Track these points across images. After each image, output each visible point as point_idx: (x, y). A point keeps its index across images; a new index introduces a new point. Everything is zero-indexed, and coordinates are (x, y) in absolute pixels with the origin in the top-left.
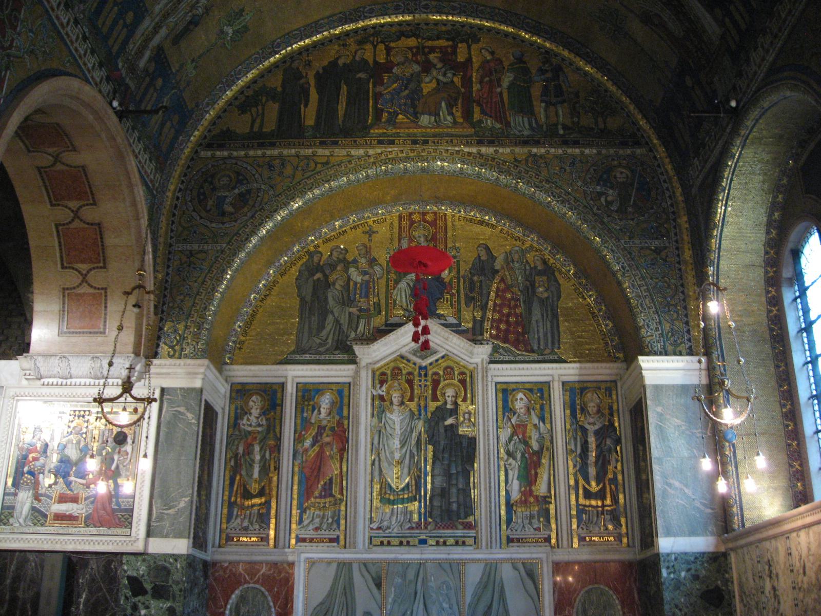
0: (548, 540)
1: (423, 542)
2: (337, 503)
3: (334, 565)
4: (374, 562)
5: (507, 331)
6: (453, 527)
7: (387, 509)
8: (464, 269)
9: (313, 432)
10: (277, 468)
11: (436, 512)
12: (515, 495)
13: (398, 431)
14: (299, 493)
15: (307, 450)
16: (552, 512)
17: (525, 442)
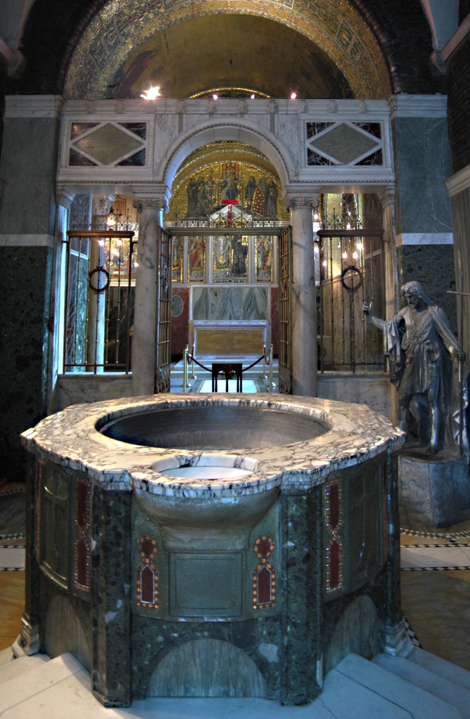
0: (270, 280)
1: (230, 281)
2: (202, 268)
3: (201, 290)
4: (216, 288)
5: (259, 209)
6: (239, 276)
7: (219, 270)
8: (245, 185)
9: (194, 245)
10: (182, 257)
11: (235, 271)
12: (260, 266)
13: (222, 245)
14: (190, 265)
15: (192, 251)
16: (272, 271)
17: (264, 248)
